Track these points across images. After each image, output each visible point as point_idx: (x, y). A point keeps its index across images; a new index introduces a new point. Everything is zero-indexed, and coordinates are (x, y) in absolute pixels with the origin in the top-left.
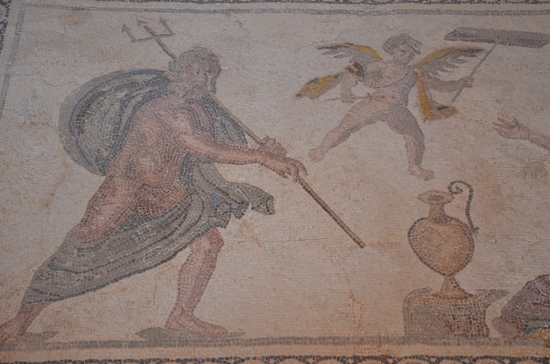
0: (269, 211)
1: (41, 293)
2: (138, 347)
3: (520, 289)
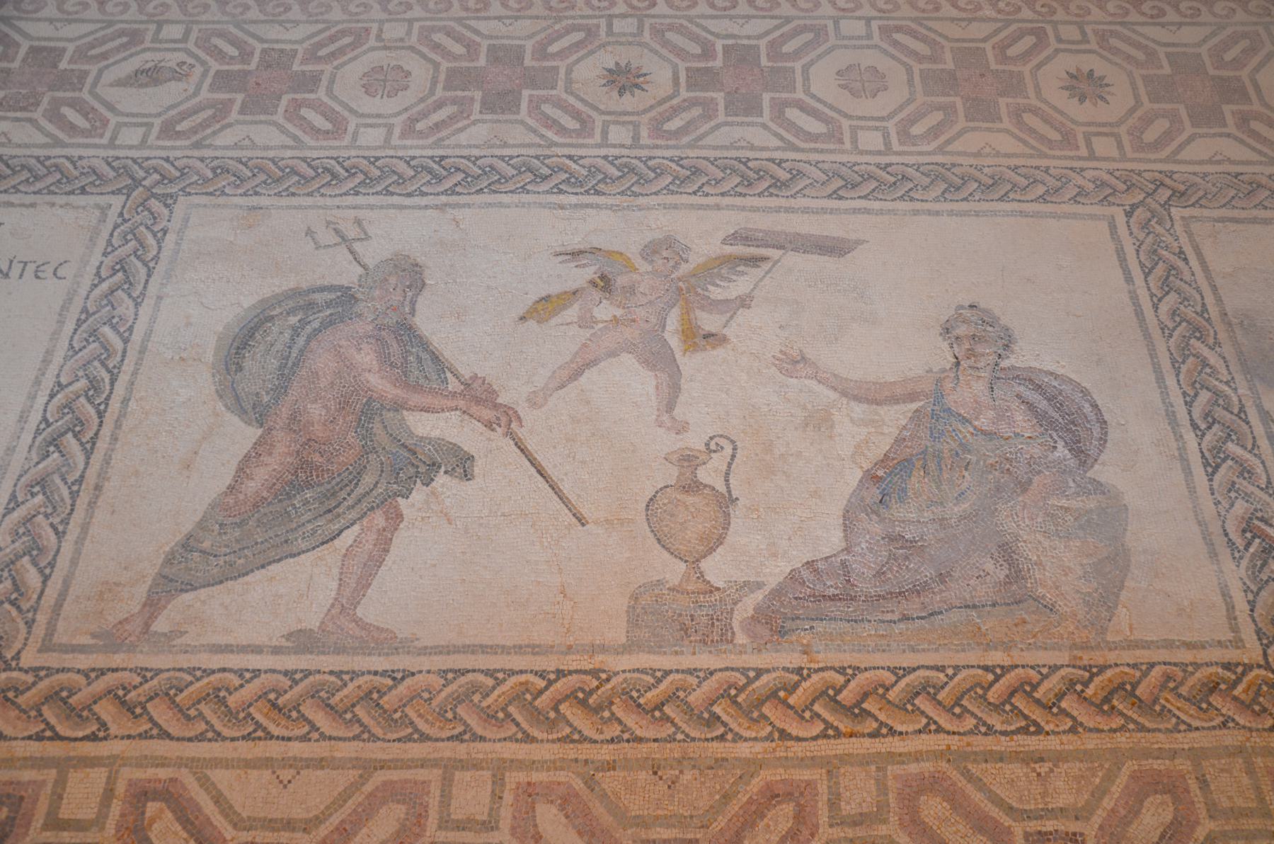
1: (171, 580)
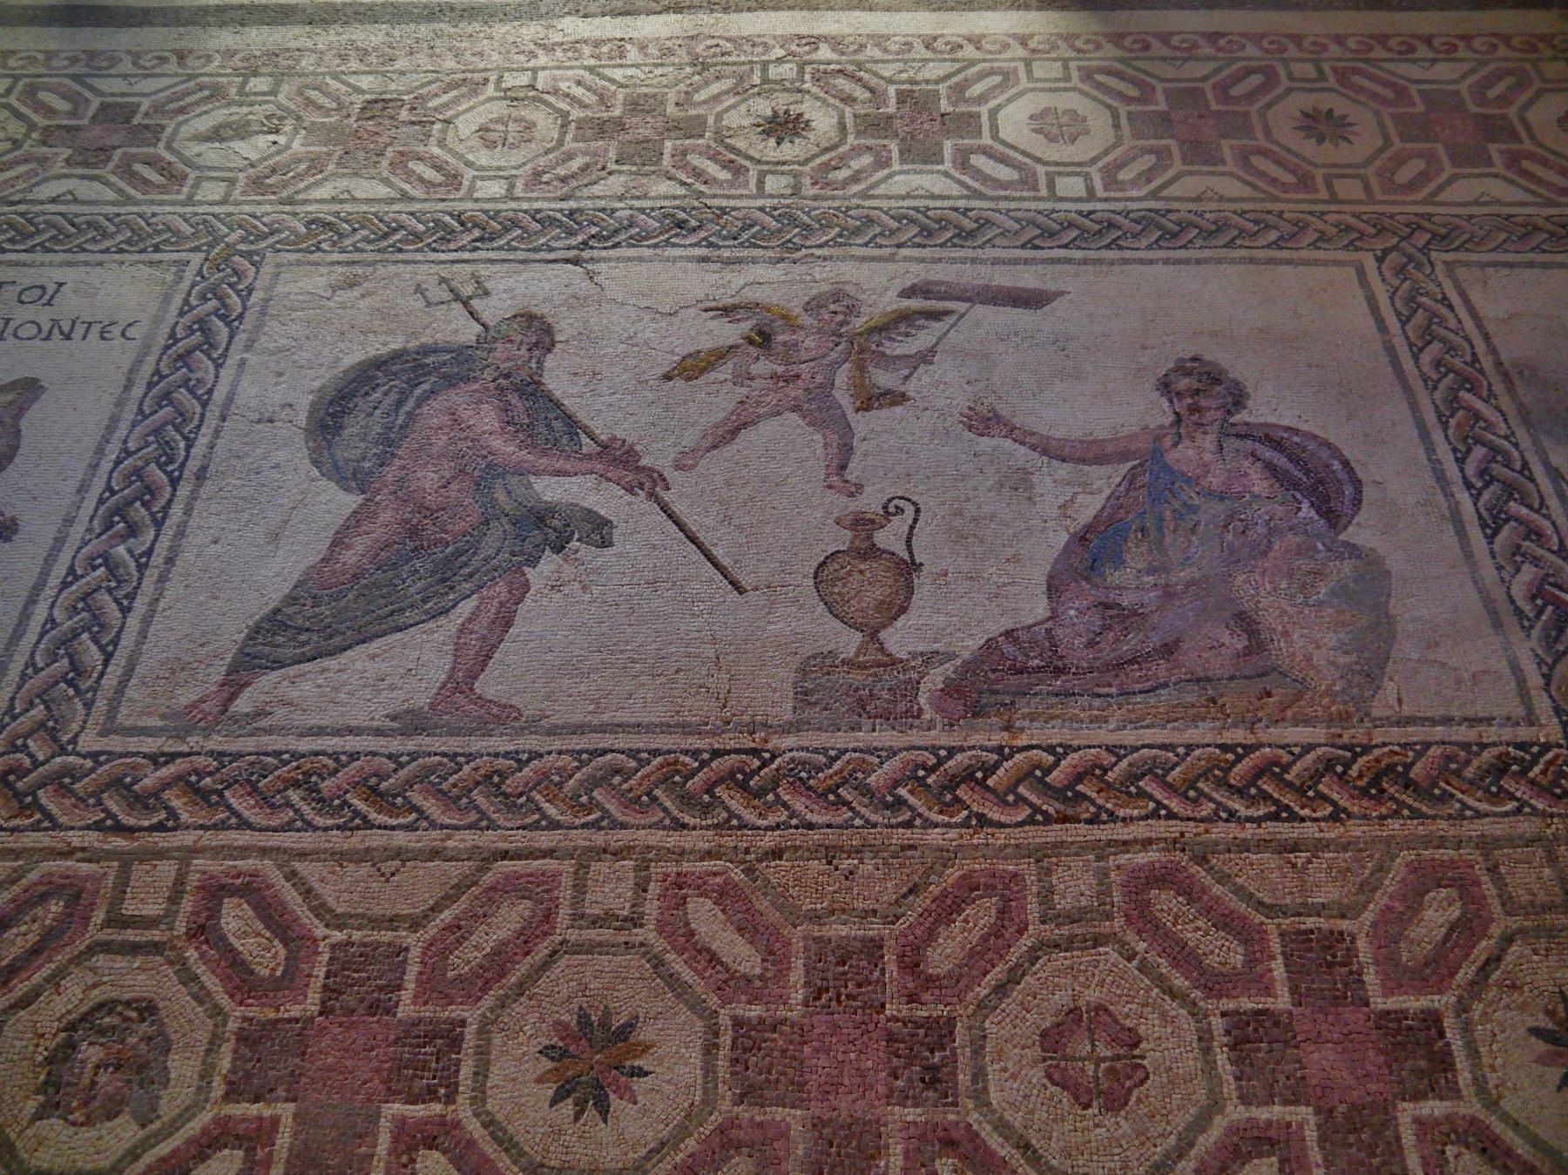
0: (606, 543)
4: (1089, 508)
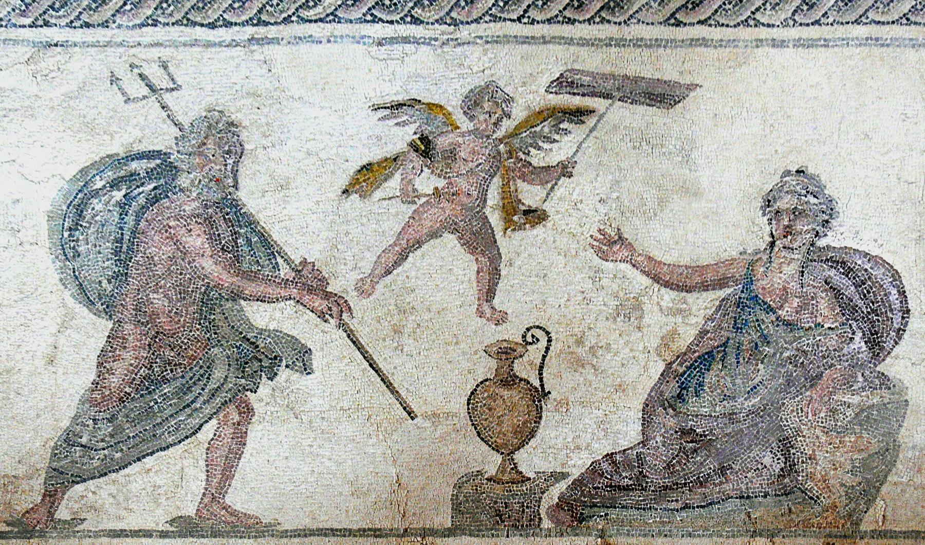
0: (307, 370)
2: (169, 537)
3: (583, 470)
4: (687, 336)
